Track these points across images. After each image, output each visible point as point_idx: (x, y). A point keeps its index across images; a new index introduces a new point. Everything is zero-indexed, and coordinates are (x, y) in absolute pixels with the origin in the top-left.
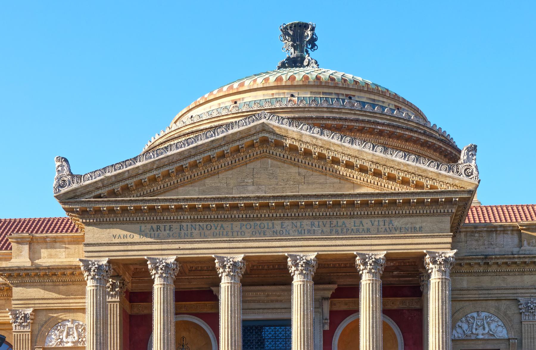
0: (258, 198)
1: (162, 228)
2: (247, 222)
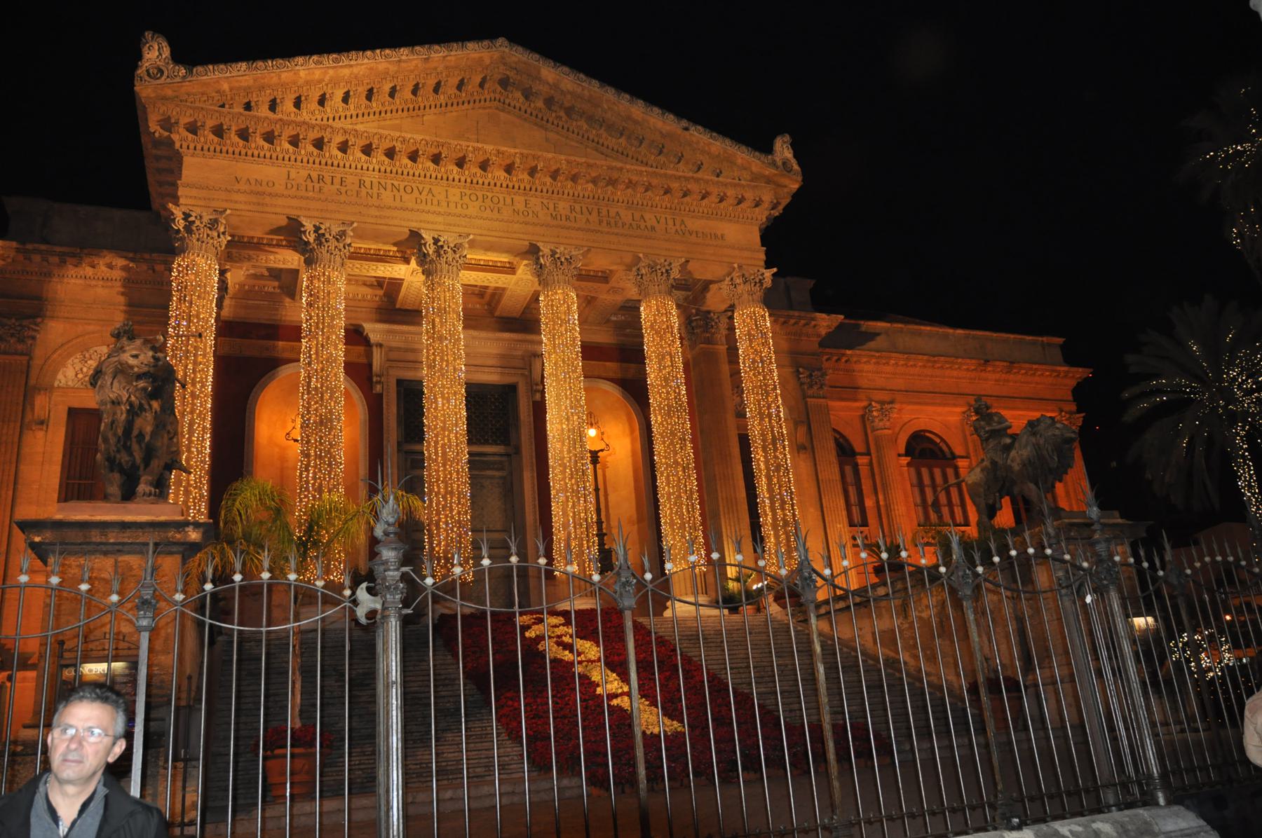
1: (328, 180)
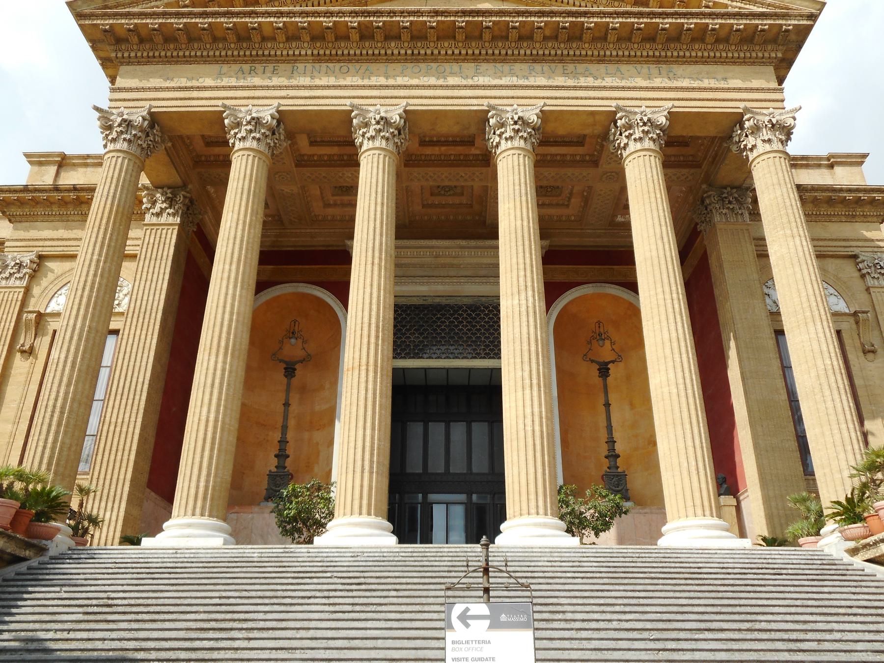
0: (437, 13)
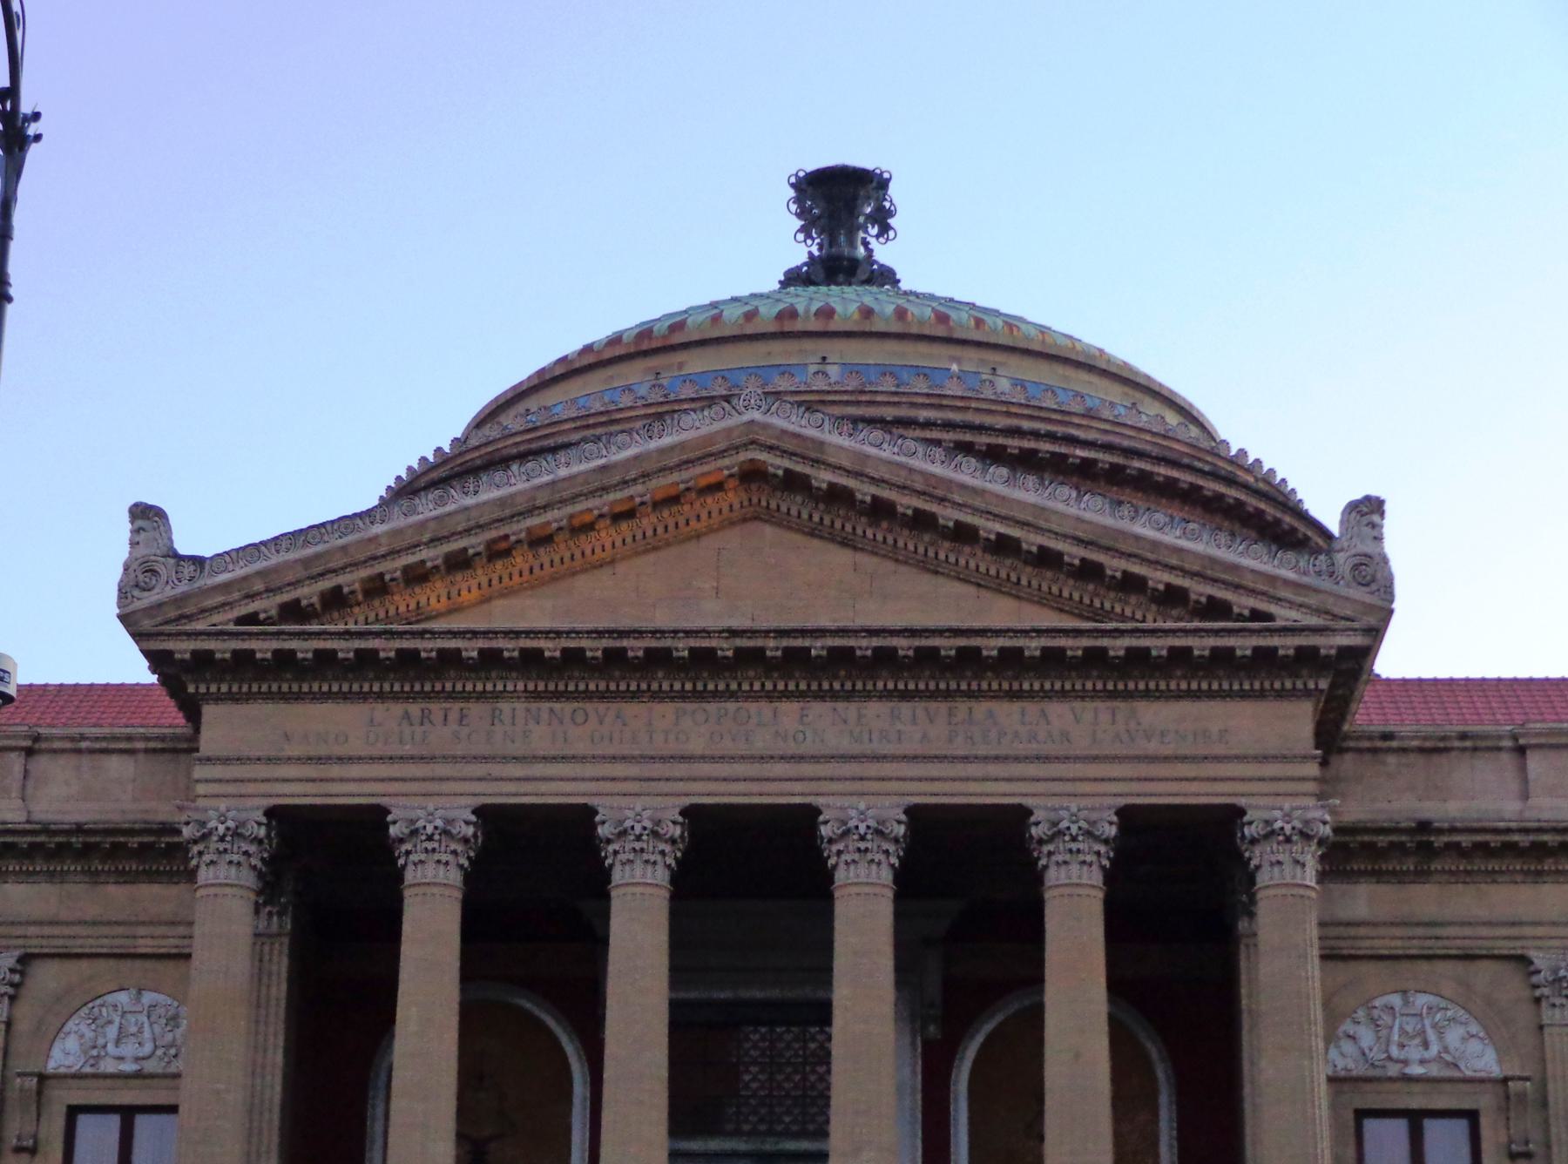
0: (733, 633)
1: (437, 716)
2: (695, 706)
